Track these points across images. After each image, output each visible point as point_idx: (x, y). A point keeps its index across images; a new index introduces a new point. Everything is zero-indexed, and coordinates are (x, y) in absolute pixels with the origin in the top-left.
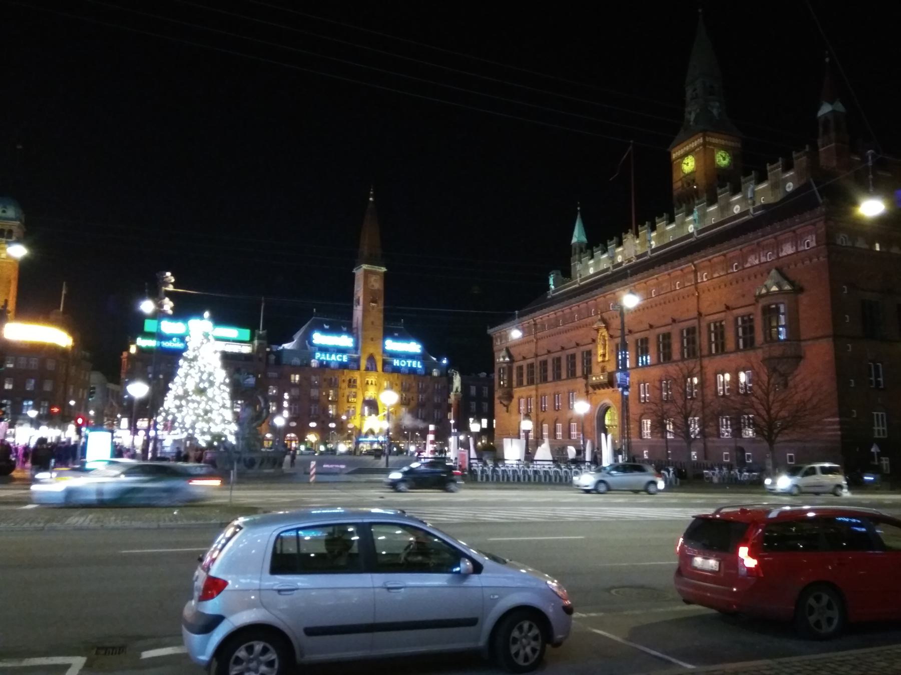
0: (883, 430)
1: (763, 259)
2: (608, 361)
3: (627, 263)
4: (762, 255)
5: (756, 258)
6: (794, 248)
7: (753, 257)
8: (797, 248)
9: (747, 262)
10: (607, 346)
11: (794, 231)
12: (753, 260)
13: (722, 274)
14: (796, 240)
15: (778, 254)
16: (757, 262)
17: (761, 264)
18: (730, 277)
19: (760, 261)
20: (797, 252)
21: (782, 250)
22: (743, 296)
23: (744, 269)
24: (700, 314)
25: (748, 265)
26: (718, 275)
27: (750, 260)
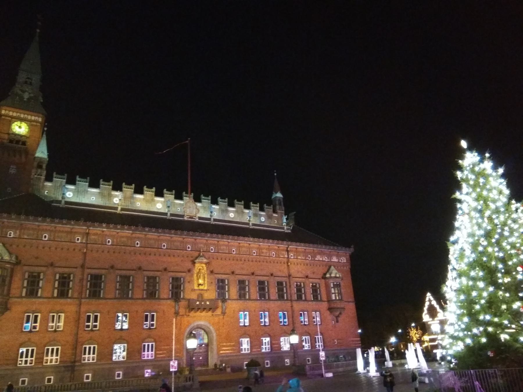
0: (321, 345)
1: (324, 259)
2: (206, 290)
3: (187, 218)
5: (321, 257)
6: (337, 260)
8: (338, 261)
10: (206, 279)
11: (338, 253)
12: (318, 258)
13: (304, 258)
14: (338, 256)
16: (321, 259)
18: (307, 261)
19: (323, 259)
20: (338, 262)
21: (332, 259)
23: (314, 260)
24: (290, 276)
25: (316, 259)
26: (300, 258)
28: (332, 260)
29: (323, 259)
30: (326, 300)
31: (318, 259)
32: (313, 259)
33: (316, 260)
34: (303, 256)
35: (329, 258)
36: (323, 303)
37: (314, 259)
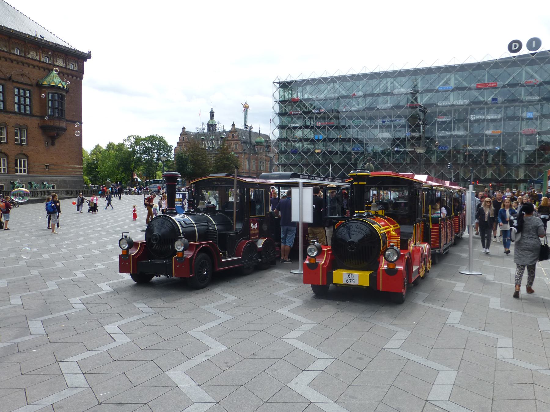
1: (42, 59)
4: (41, 56)
5: (37, 56)
6: (65, 64)
7: (35, 53)
8: (66, 66)
9: (29, 53)
13: (5, 50)
15: (53, 62)
16: (37, 58)
17: (39, 61)
19: (40, 58)
20: (66, 68)
21: (56, 61)
22: (22, 75)
23: (25, 57)
25: (30, 56)
27: (31, 53)
28: (55, 63)
29: (40, 58)
30: (38, 114)
31: (31, 57)
32: (23, 55)
33: (29, 58)
34: (6, 47)
35: (52, 59)
36: (34, 118)
37: (25, 55)
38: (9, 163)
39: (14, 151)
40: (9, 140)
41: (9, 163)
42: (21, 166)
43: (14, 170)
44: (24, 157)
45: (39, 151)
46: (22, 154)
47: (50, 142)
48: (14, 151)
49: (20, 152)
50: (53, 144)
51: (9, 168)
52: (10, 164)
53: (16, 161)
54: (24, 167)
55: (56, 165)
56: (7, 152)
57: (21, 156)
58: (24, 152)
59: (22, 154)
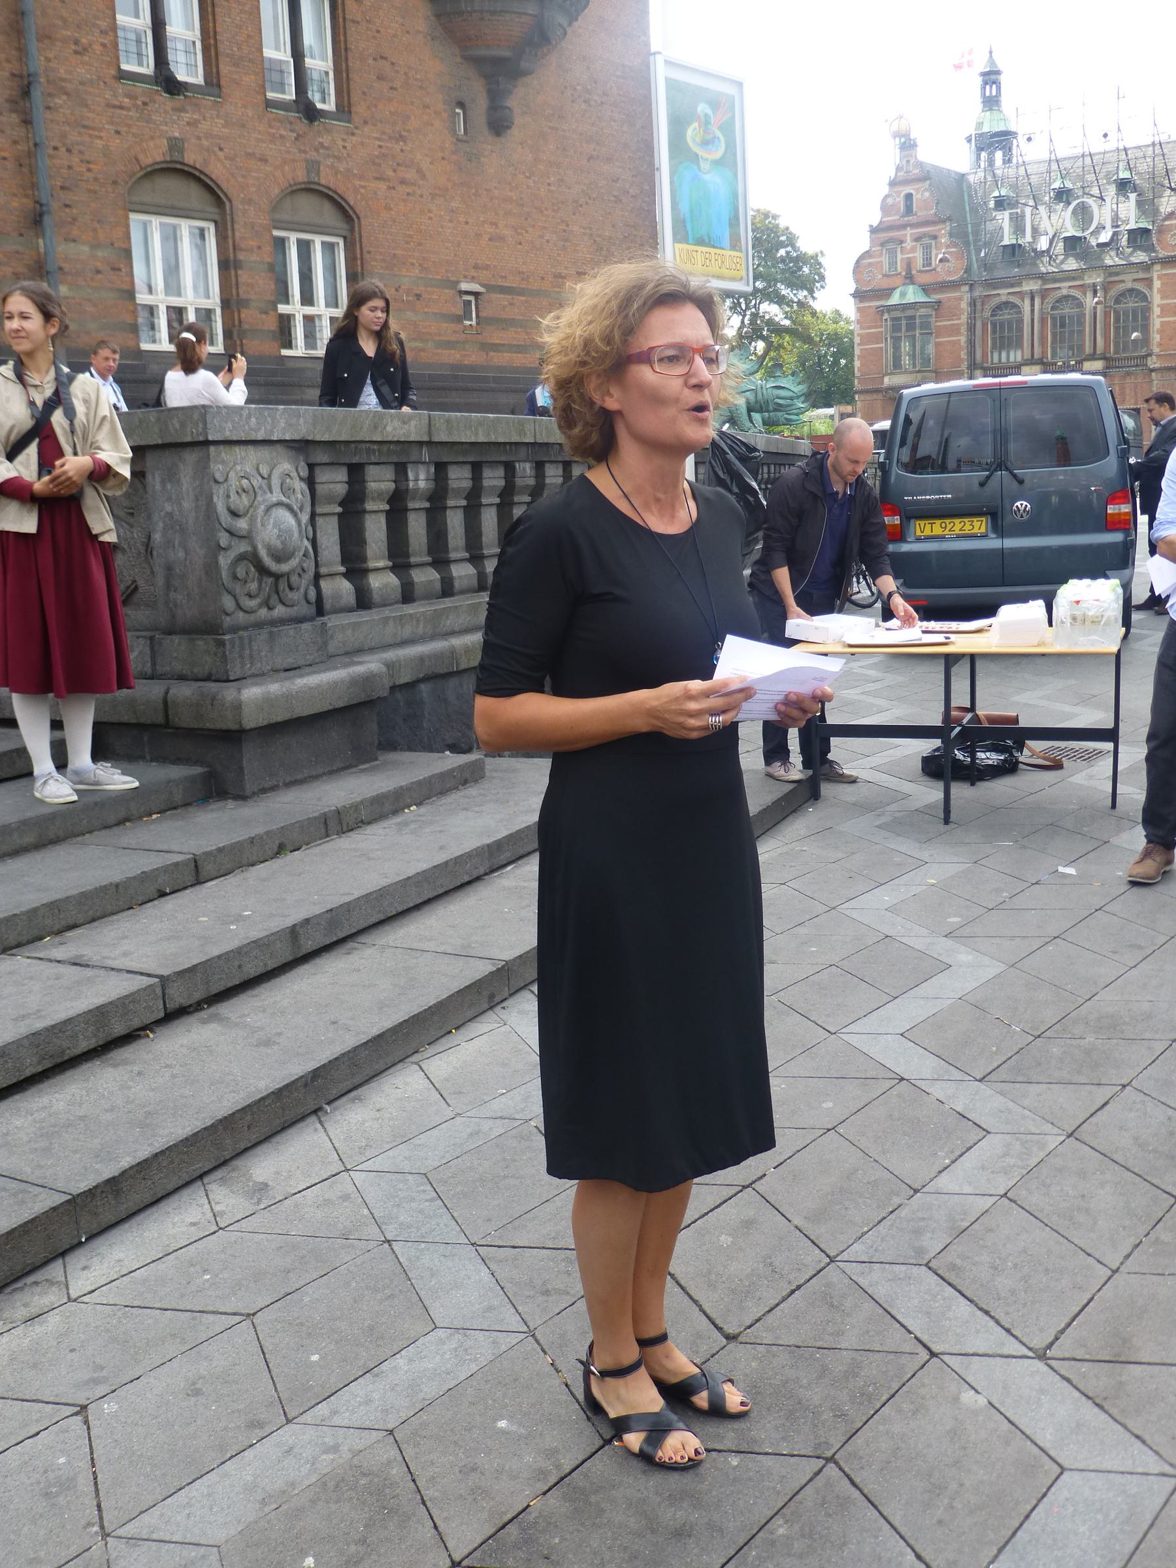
38: (238, 265)
39: (263, 160)
40: (225, 69)
41: (238, 265)
42: (308, 298)
43: (272, 324)
44: (328, 214)
45: (419, 171)
46: (312, 190)
47: (481, 105)
48: (263, 160)
49: (301, 176)
50: (499, 125)
51: (243, 303)
52: (244, 277)
53: (281, 243)
54: (333, 302)
55: (520, 292)
56: (217, 170)
57: (308, 207)
58: (326, 178)
59: (312, 190)
